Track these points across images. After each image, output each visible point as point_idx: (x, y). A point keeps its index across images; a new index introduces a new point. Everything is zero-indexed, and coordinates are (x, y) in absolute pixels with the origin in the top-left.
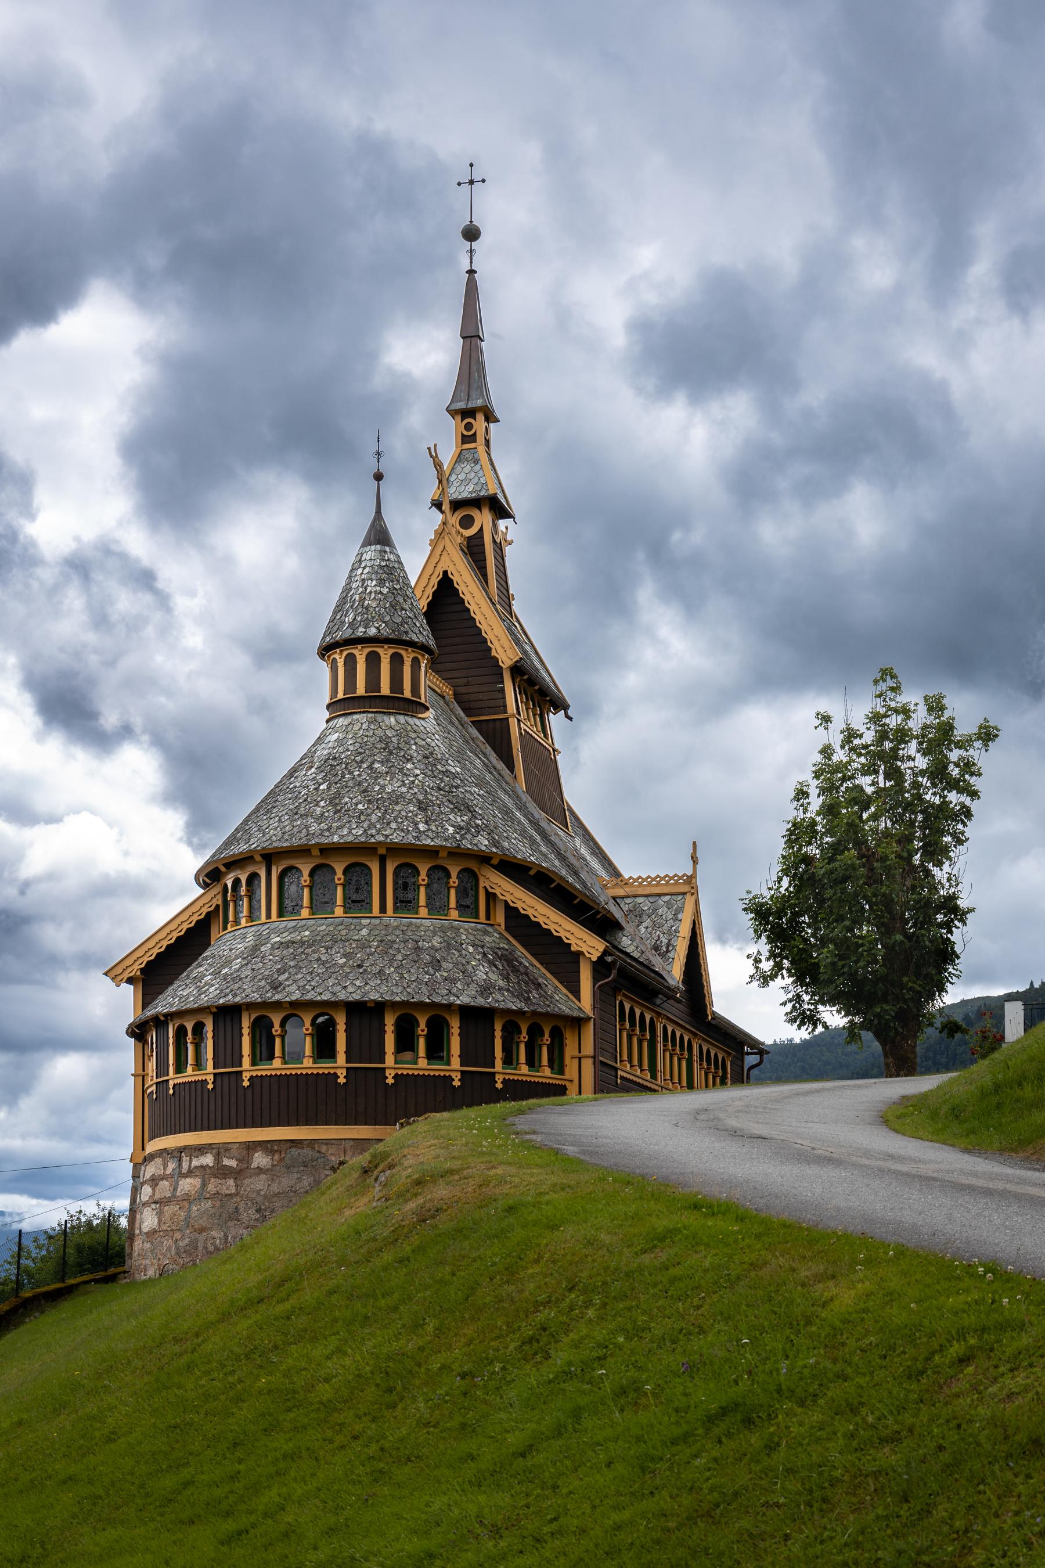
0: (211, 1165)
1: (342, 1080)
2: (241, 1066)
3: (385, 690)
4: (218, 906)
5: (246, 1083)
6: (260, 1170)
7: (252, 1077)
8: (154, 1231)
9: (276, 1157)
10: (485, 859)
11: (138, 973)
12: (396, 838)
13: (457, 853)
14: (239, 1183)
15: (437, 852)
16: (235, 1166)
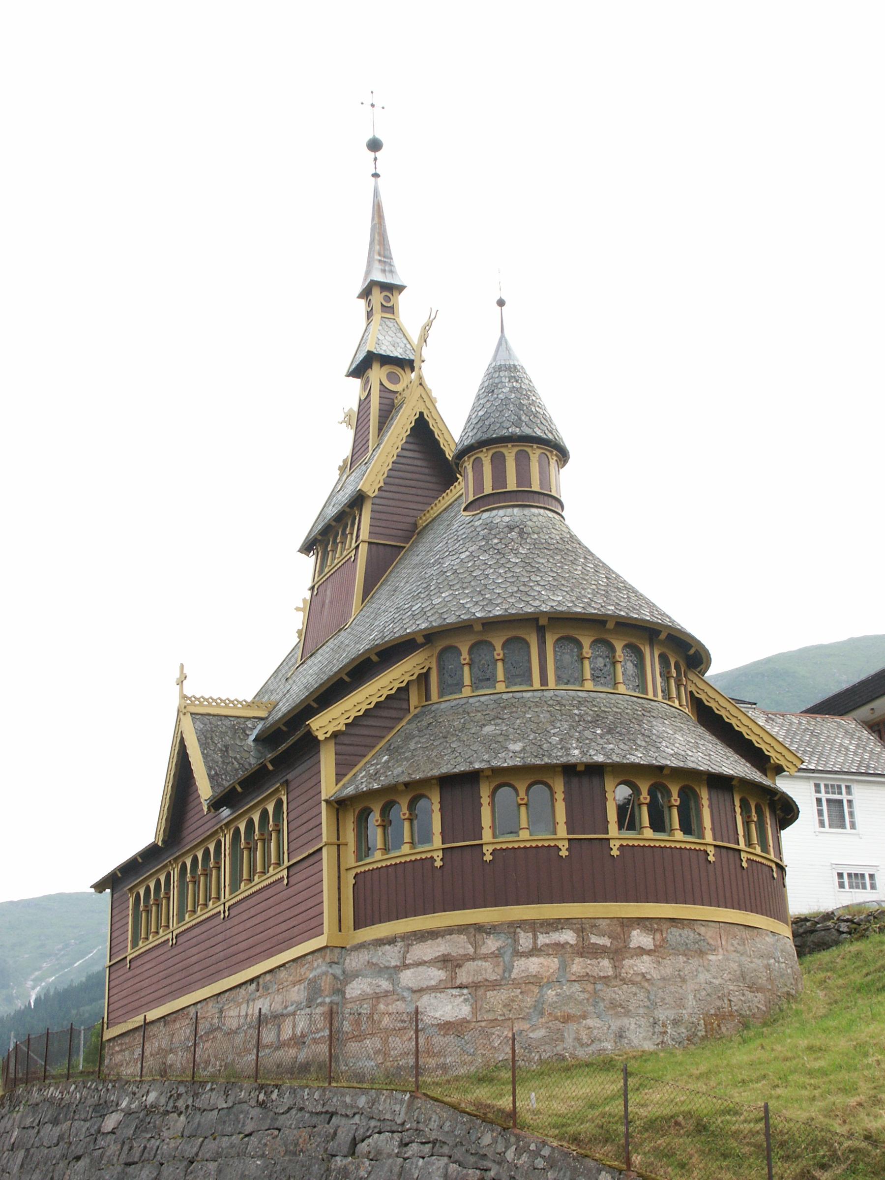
0: (573, 942)
6: (642, 951)
8: (464, 1022)
9: (658, 936)
14: (617, 964)
16: (609, 945)
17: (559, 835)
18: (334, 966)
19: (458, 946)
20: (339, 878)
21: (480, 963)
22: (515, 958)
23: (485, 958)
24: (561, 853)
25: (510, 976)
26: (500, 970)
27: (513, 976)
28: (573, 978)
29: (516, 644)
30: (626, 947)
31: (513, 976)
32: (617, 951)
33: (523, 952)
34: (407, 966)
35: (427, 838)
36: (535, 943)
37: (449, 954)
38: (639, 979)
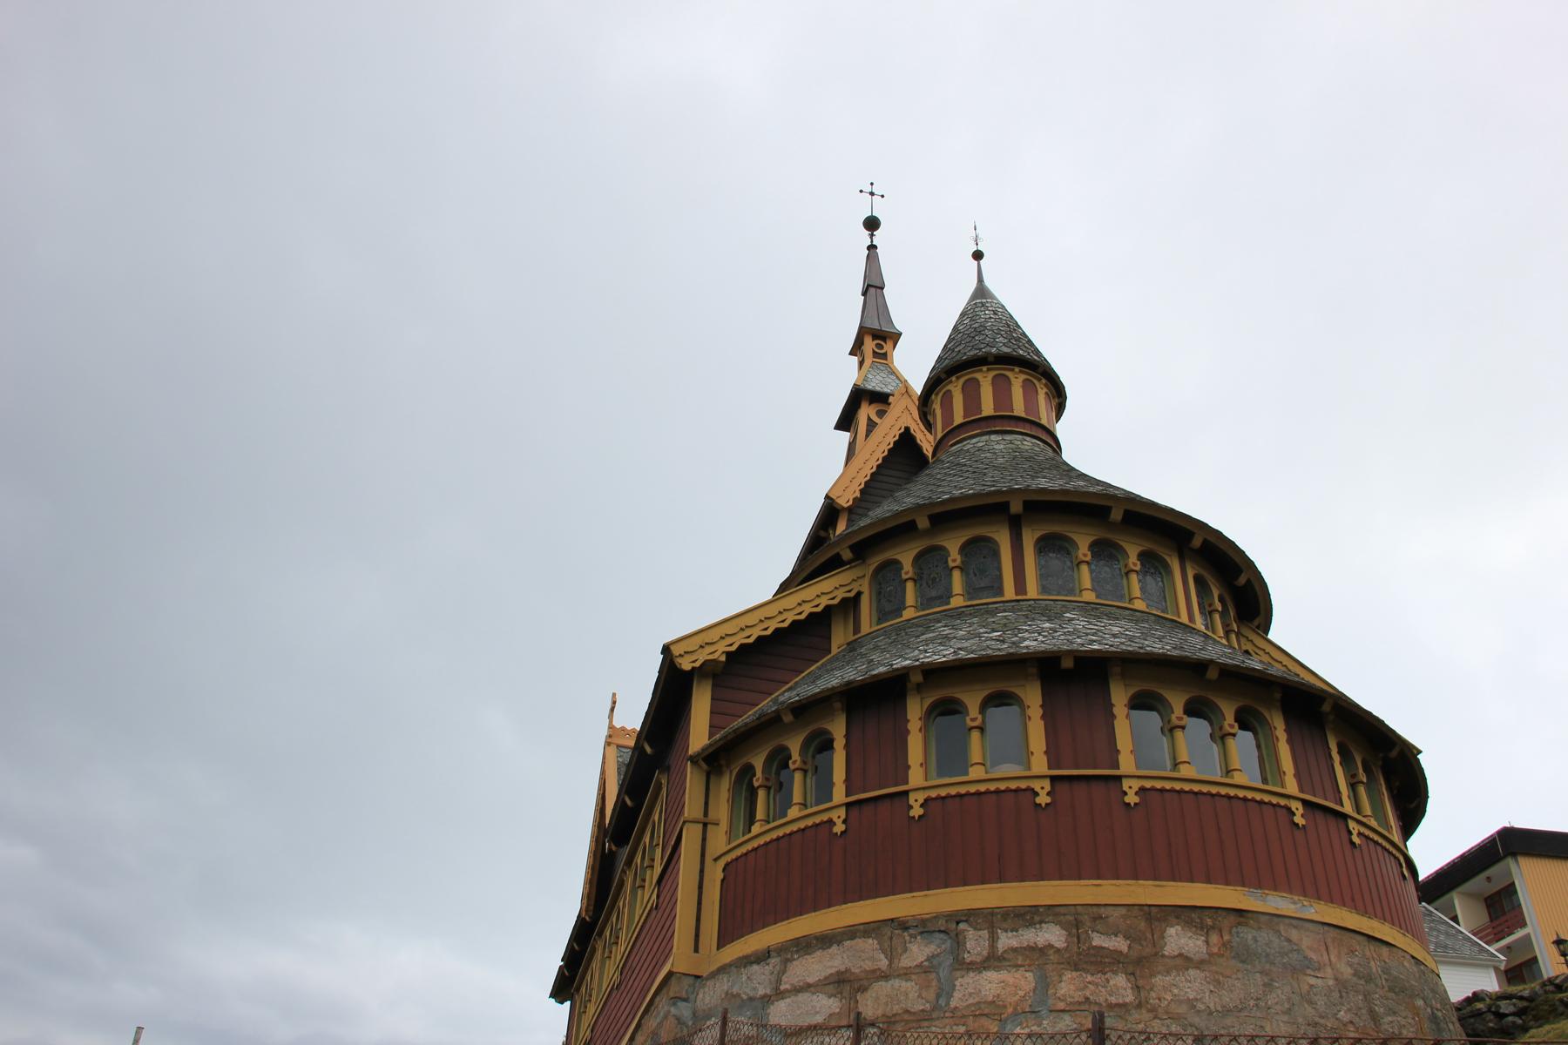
0: (1057, 945)
4: (859, 594)
6: (1185, 962)
7: (1142, 790)
9: (1214, 938)
11: (723, 658)
14: (1140, 983)
16: (1125, 949)
17: (1036, 770)
18: (680, 1004)
19: (864, 955)
20: (702, 871)
21: (896, 982)
22: (958, 973)
23: (906, 974)
24: (1038, 800)
25: (948, 1004)
26: (931, 995)
27: (953, 1004)
28: (1061, 1005)
29: (979, 551)
30: (1156, 954)
31: (953, 1004)
32: (1139, 961)
33: (971, 963)
34: (779, 994)
35: (825, 792)
36: (993, 946)
37: (848, 970)
38: (1182, 1009)
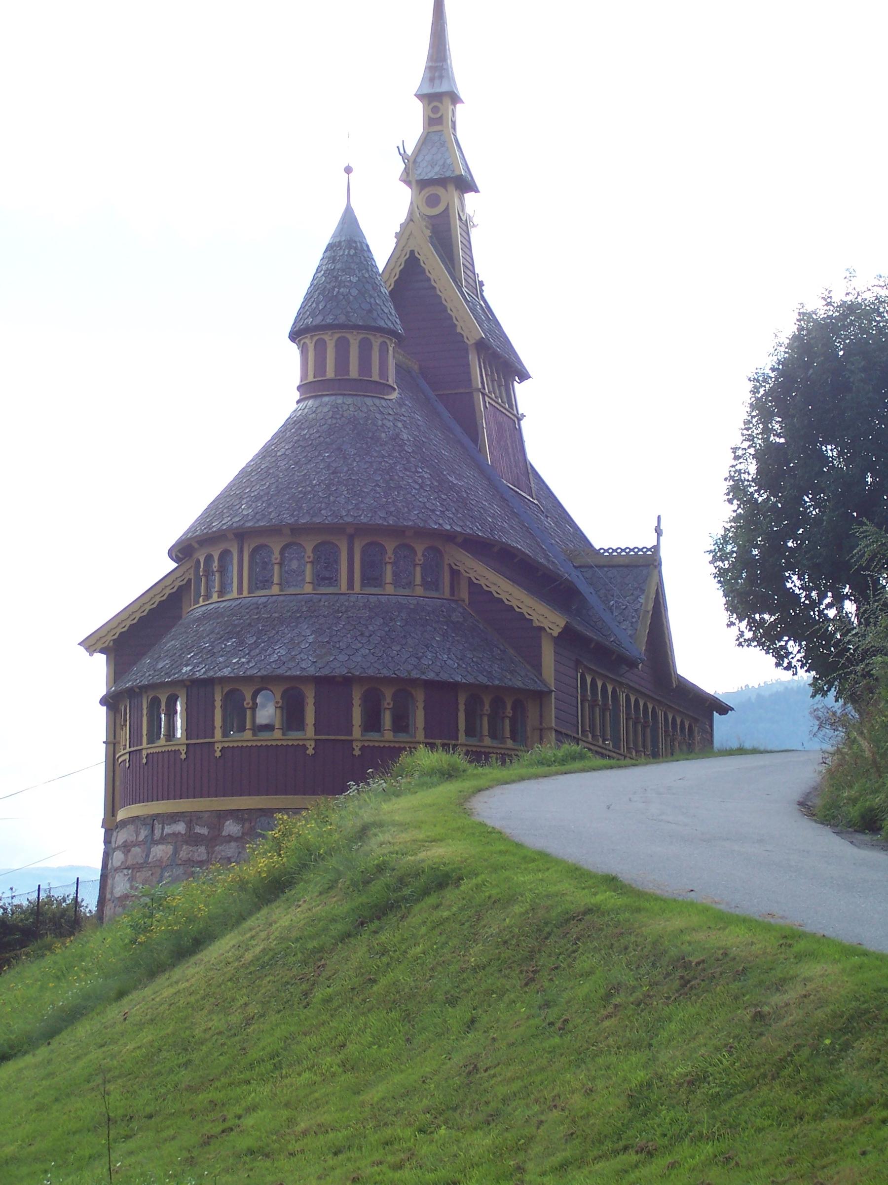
0: (183, 832)
1: (310, 751)
2: (213, 737)
3: (354, 373)
4: (190, 580)
5: (218, 754)
6: (231, 838)
8: (126, 897)
9: (247, 825)
10: (450, 537)
12: (363, 519)
13: (421, 533)
15: (404, 532)
16: (206, 833)
28: (180, 862)
36: (162, 833)
